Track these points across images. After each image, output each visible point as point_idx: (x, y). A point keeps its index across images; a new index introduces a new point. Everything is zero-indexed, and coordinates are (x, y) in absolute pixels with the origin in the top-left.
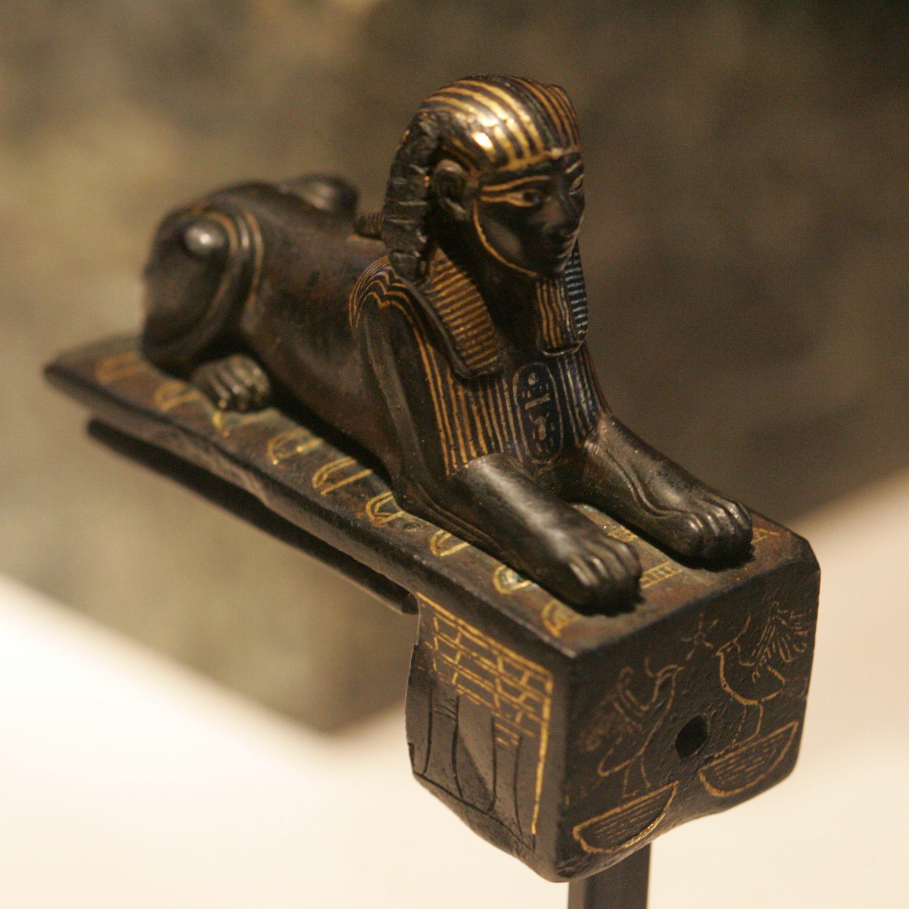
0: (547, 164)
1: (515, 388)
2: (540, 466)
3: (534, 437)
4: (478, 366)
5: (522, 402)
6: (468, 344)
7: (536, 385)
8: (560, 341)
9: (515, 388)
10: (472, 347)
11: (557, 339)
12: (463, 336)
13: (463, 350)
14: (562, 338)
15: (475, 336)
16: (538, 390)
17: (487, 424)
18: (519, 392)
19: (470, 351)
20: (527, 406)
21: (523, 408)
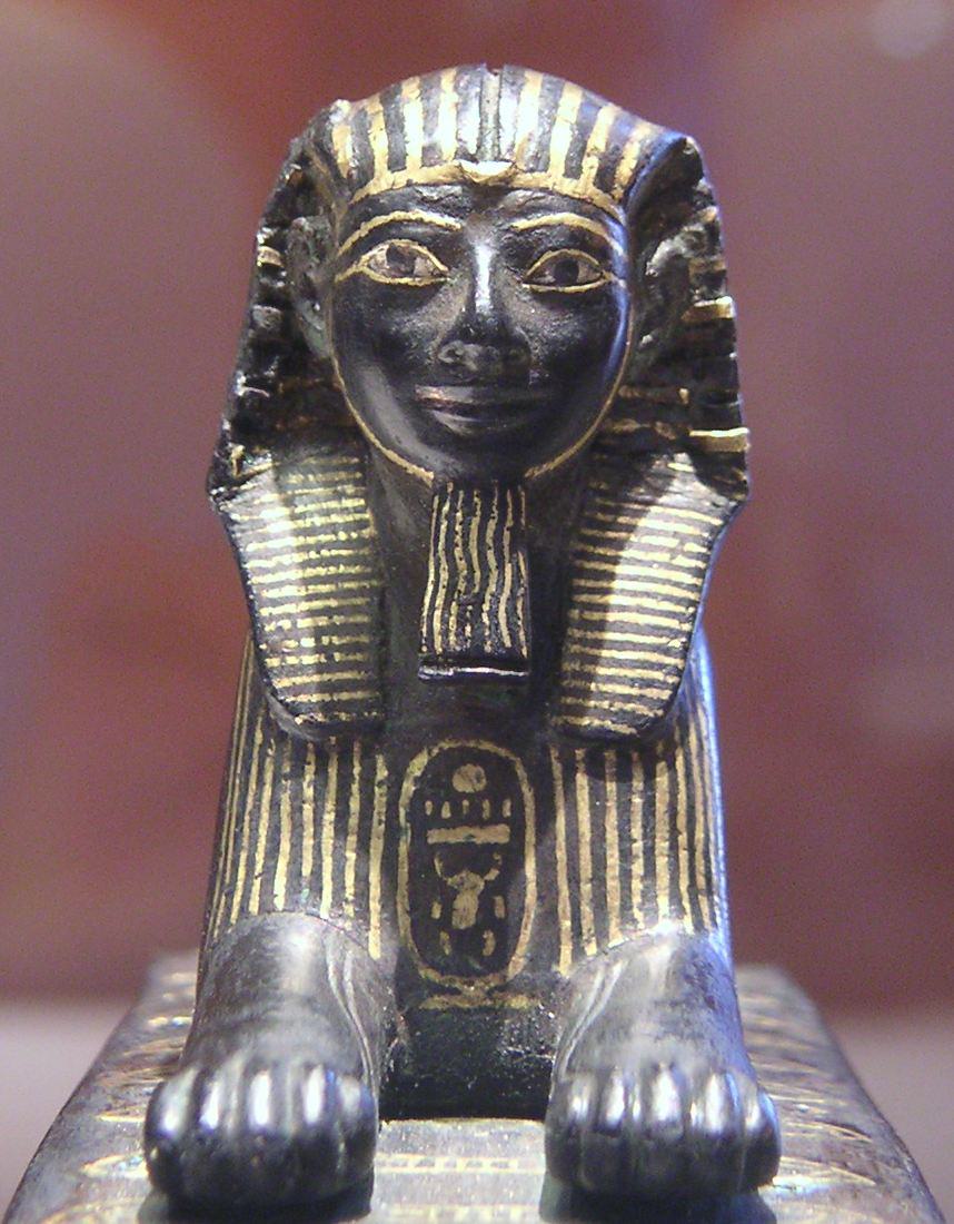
0: (457, 189)
1: (409, 787)
2: (439, 990)
3: (437, 914)
4: (303, 698)
5: (421, 824)
6: (292, 644)
7: (476, 798)
8: (452, 638)
9: (409, 787)
10: (300, 651)
11: (445, 633)
12: (286, 624)
13: (275, 652)
14: (460, 633)
15: (318, 633)
16: (476, 808)
17: (308, 842)
18: (418, 798)
19: (291, 660)
20: (435, 837)
21: (419, 835)
